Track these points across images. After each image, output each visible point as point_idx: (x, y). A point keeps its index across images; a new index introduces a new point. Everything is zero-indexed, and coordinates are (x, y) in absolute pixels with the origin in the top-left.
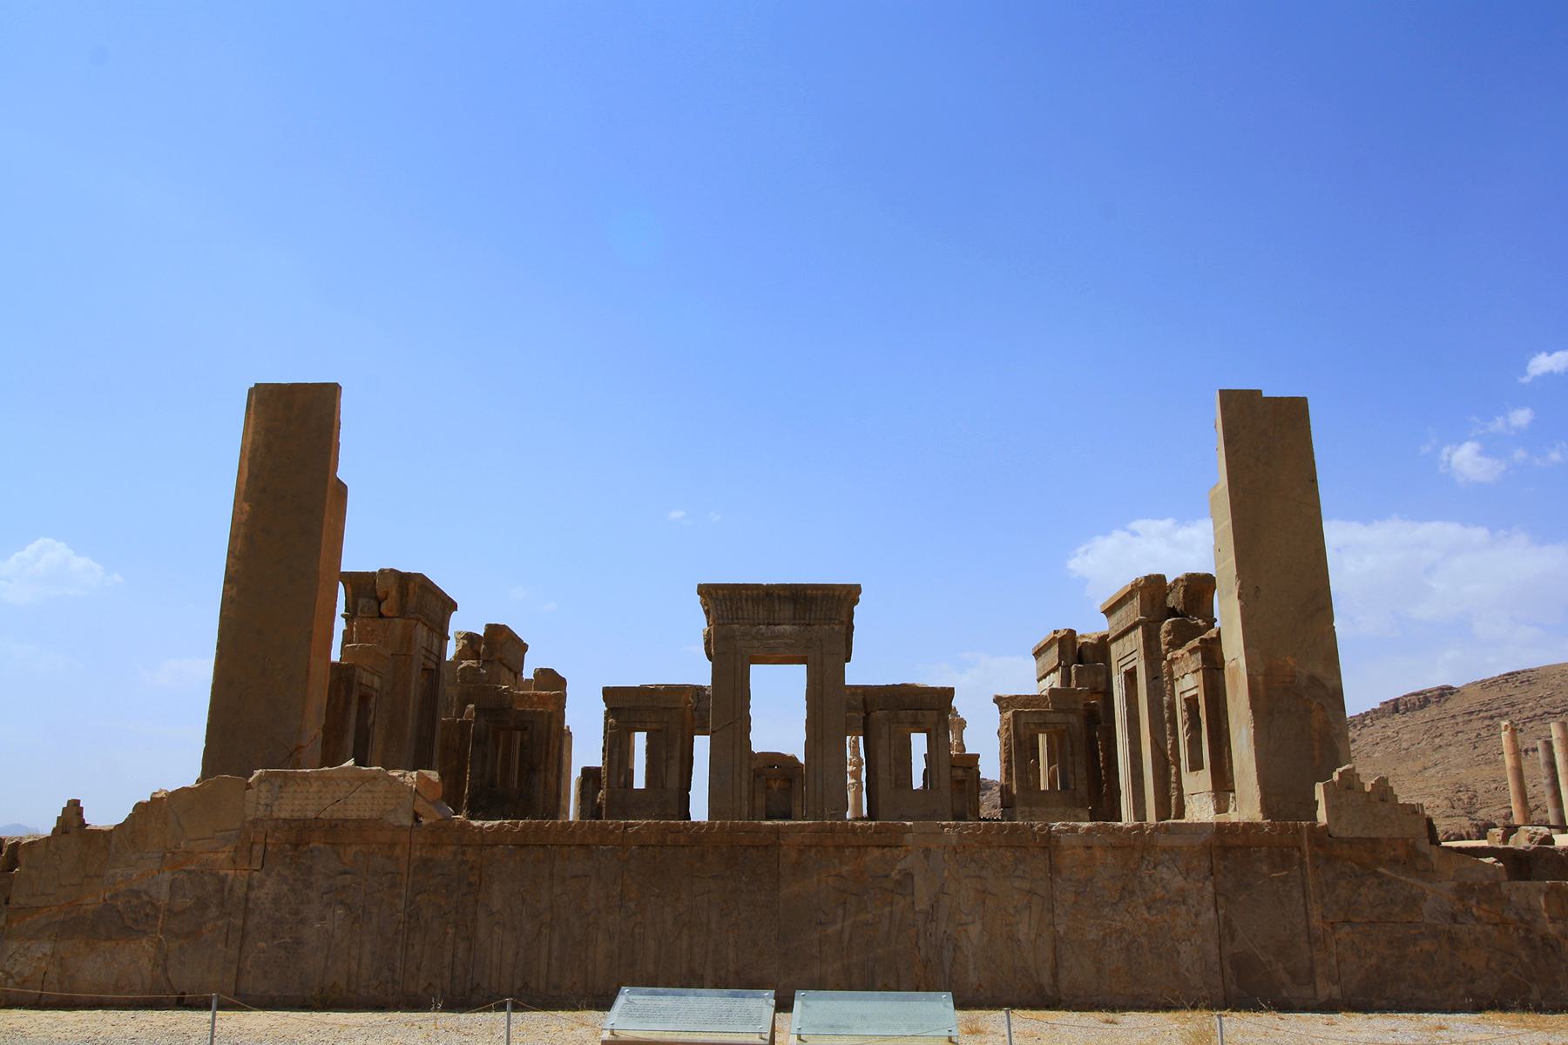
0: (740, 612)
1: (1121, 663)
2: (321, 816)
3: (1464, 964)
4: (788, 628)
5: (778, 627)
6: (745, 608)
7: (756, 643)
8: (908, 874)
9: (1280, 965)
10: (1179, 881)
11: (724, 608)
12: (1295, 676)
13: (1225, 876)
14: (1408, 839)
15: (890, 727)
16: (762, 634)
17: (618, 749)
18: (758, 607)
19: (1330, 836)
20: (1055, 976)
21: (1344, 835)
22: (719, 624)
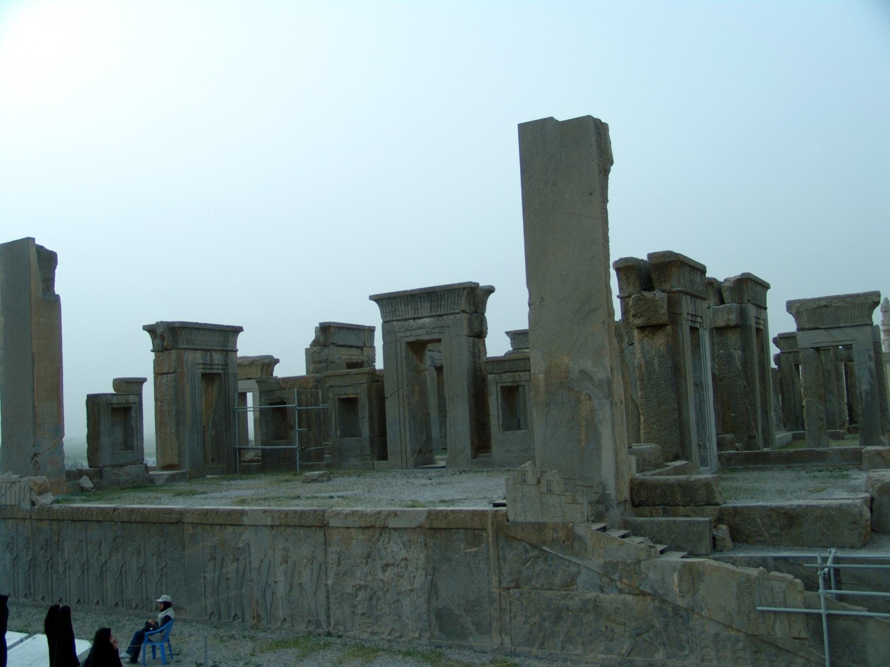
0: (397, 312)
3: (607, 627)
4: (427, 320)
5: (421, 320)
6: (400, 309)
7: (408, 333)
8: (247, 543)
10: (403, 554)
11: (388, 311)
12: (569, 372)
13: (434, 551)
14: (568, 523)
15: (497, 387)
16: (411, 326)
17: (334, 413)
18: (408, 307)
19: (508, 520)
20: (328, 617)
21: (519, 519)
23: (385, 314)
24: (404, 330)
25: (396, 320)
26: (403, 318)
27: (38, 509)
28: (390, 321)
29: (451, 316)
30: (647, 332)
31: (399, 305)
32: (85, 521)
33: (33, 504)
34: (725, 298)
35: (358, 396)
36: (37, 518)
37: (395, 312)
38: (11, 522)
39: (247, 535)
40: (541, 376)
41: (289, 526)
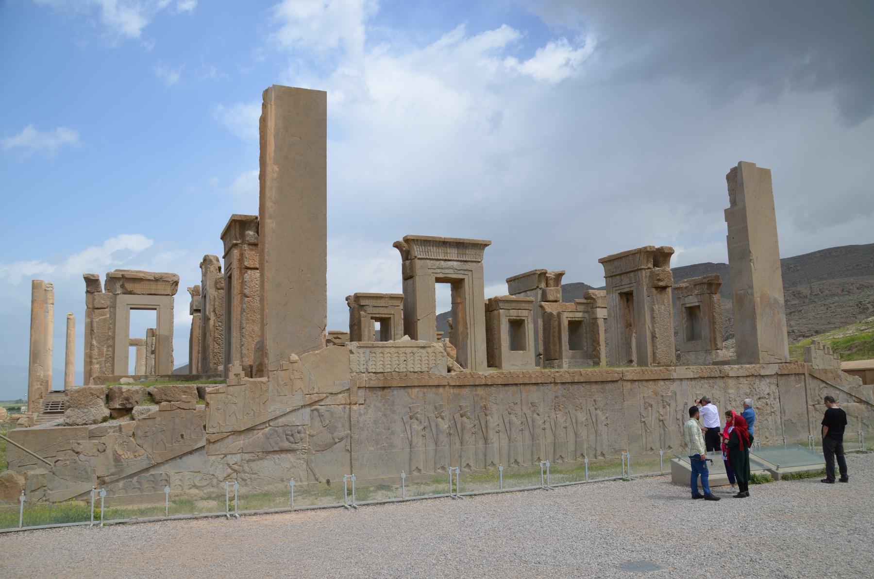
0: (430, 253)
1: (614, 289)
2: (397, 370)
4: (455, 263)
5: (449, 262)
6: (432, 250)
7: (439, 271)
9: (799, 425)
11: (421, 250)
22: (419, 259)
23: (419, 252)
24: (435, 268)
25: (430, 259)
26: (436, 258)
27: (457, 375)
28: (424, 259)
29: (474, 264)
30: (659, 290)
31: (432, 248)
32: (520, 384)
33: (449, 371)
34: (550, 284)
35: (391, 316)
36: (458, 384)
37: (428, 253)
38: (415, 390)
39: (674, 386)
40: (759, 299)
41: (704, 378)
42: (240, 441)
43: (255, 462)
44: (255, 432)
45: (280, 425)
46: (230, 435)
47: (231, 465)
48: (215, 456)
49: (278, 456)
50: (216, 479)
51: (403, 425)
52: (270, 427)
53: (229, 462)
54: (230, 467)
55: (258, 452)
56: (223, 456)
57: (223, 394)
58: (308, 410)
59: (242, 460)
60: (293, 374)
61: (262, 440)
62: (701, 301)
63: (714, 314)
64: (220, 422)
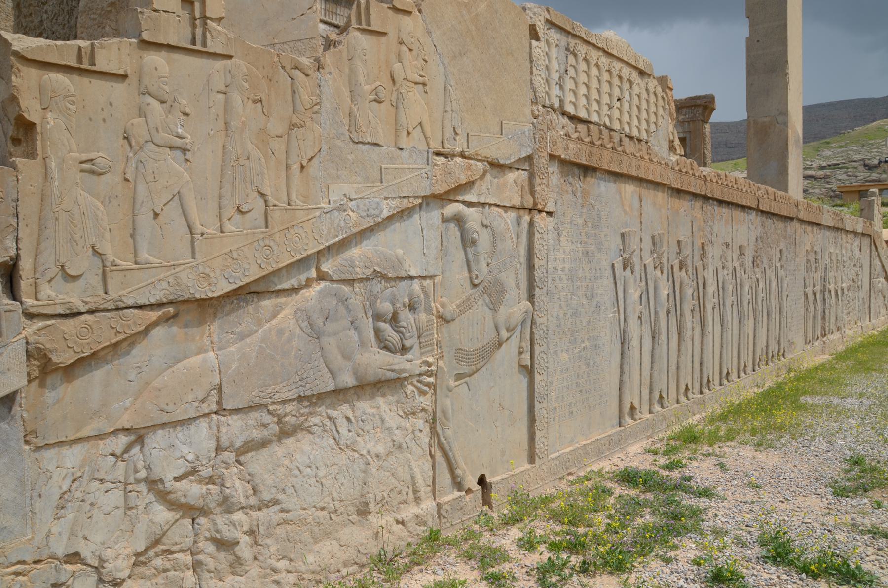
42: (201, 351)
43: (265, 452)
44: (267, 303)
45: (360, 273)
46: (155, 324)
47: (169, 484)
48: (77, 449)
49: (345, 409)
50: (94, 577)
51: (612, 285)
52: (323, 284)
53: (157, 474)
54: (164, 497)
55: (284, 402)
56: (123, 440)
57: (118, 89)
58: (434, 216)
59: (219, 449)
60: (400, 61)
61: (295, 343)
62: (690, 132)
63: (706, 151)
64: (107, 249)
